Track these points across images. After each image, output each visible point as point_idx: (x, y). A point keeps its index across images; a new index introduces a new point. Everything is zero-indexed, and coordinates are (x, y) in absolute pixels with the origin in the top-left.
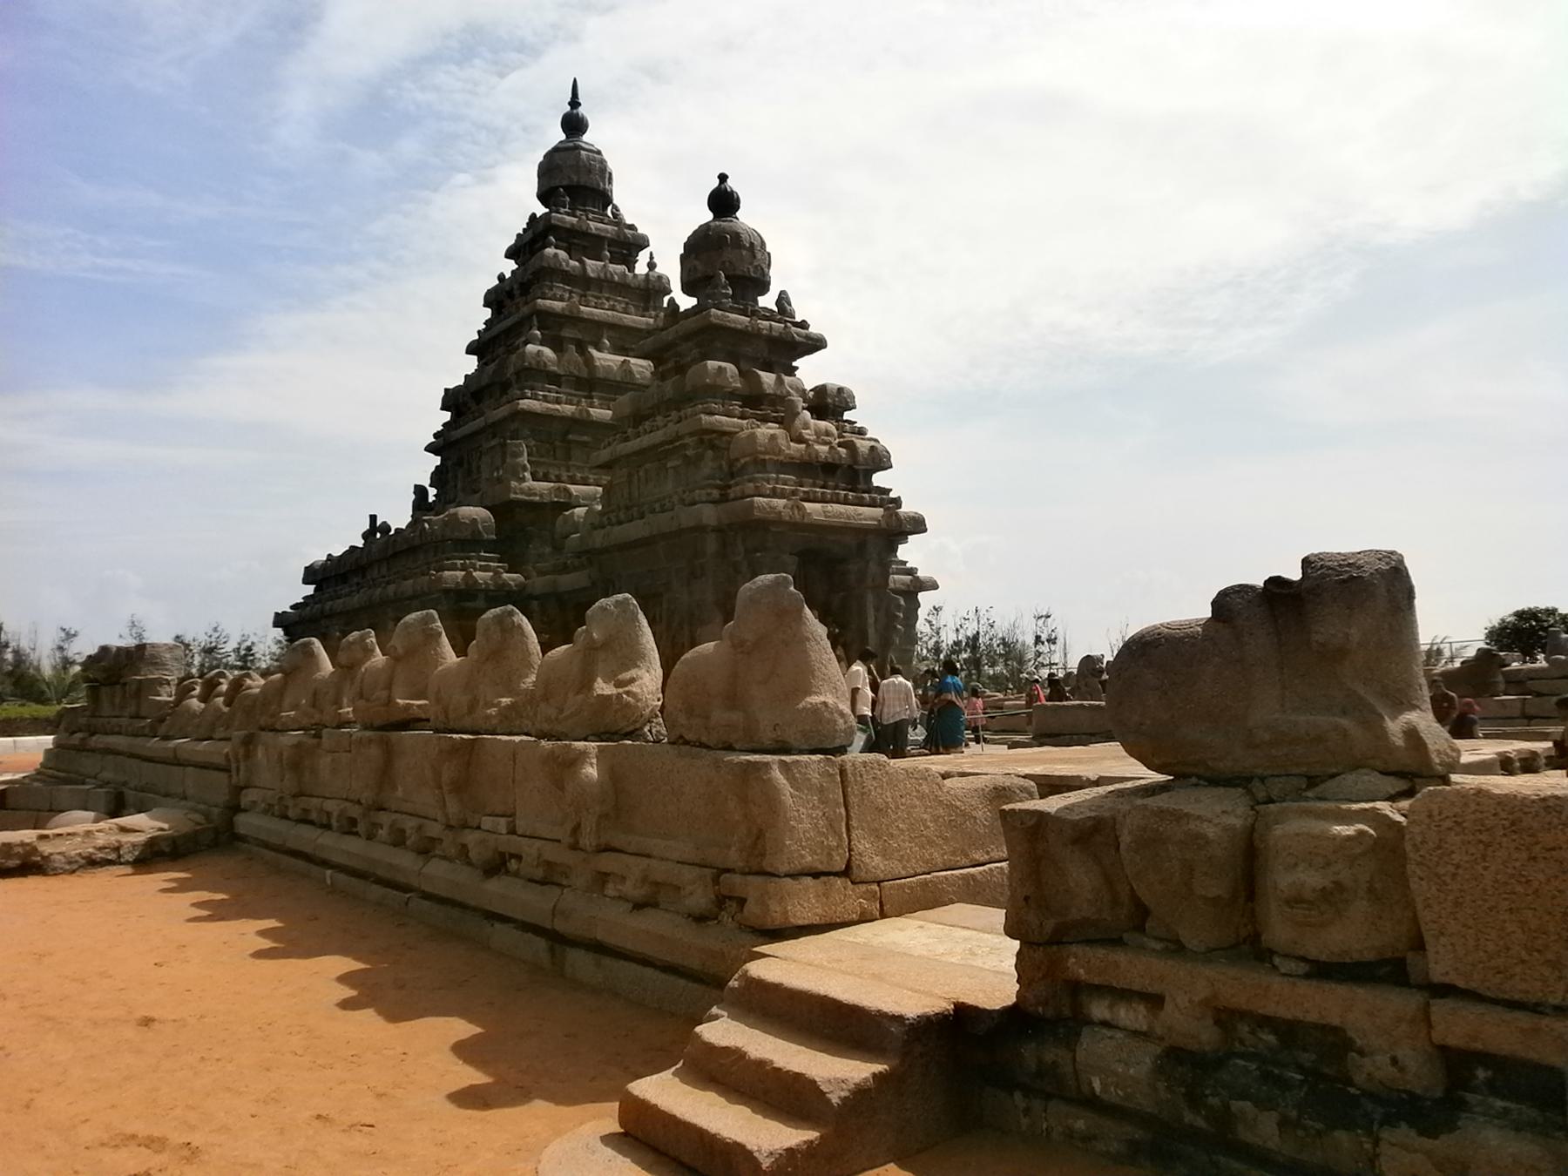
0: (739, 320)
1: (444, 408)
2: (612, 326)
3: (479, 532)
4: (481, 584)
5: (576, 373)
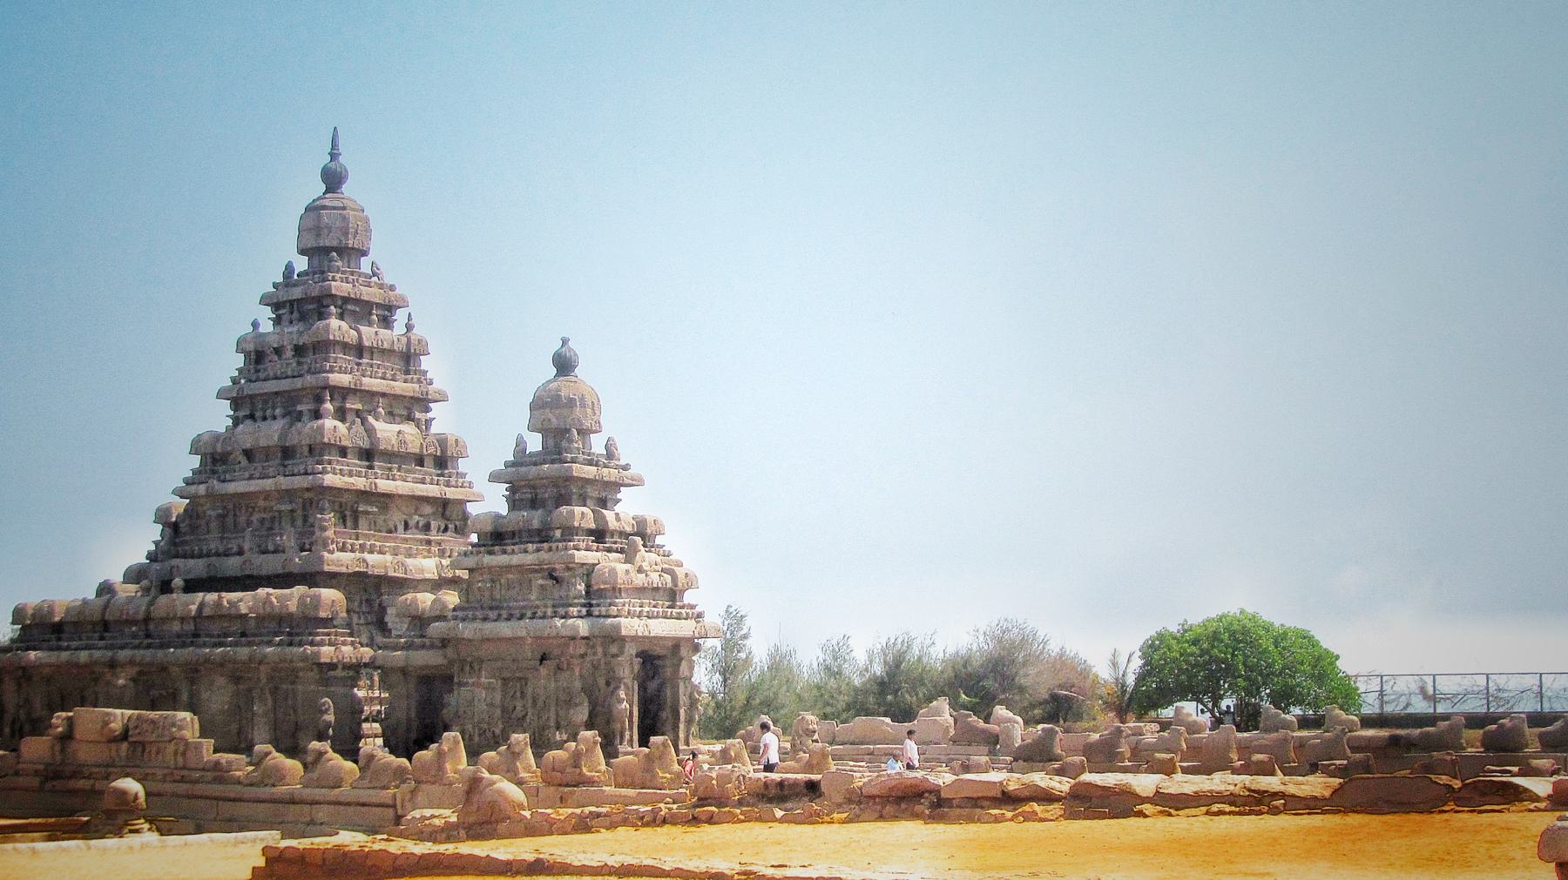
0: (590, 472)
2: (384, 395)
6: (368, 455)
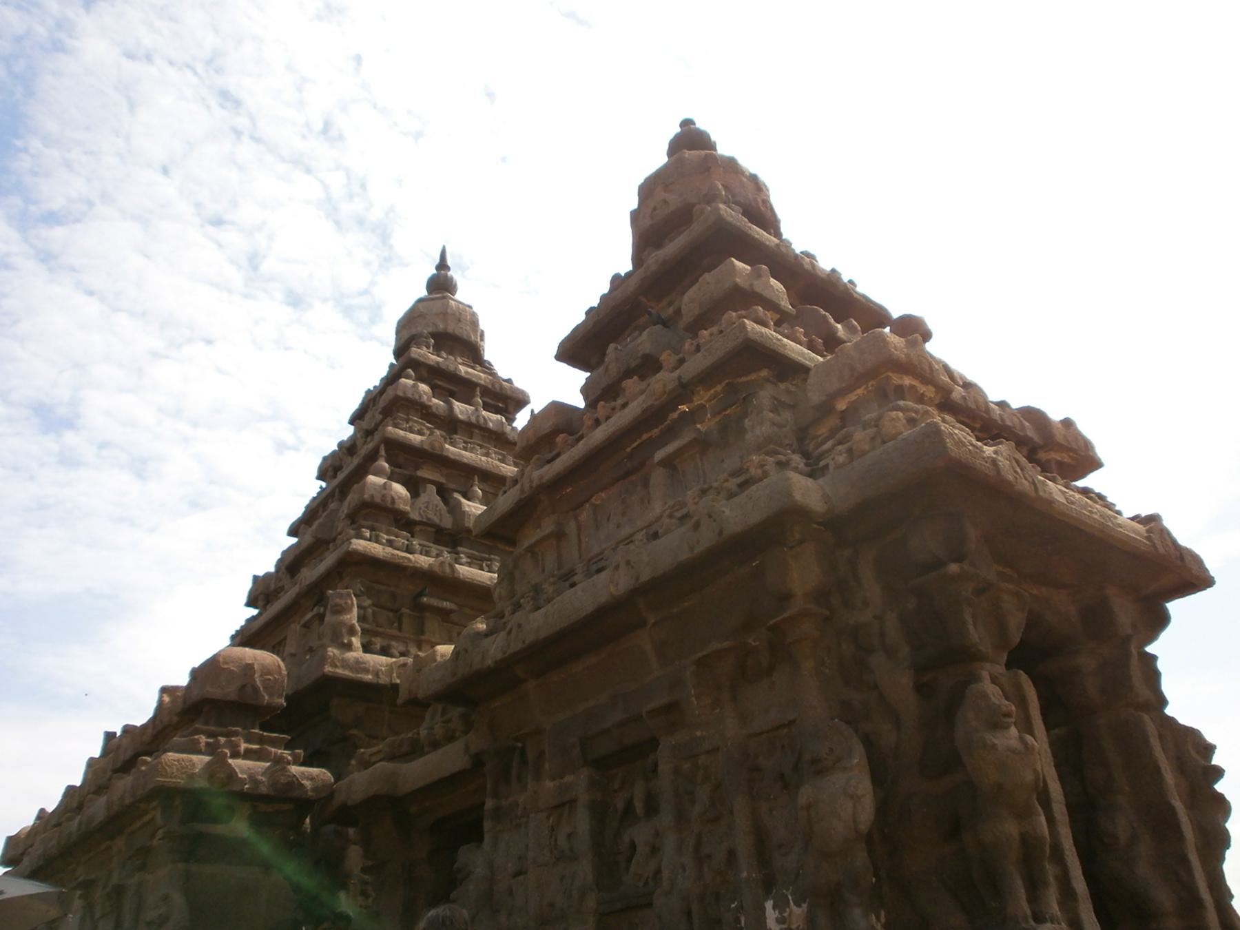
1: (251, 603)
3: (255, 689)
4: (243, 781)
5: (436, 520)
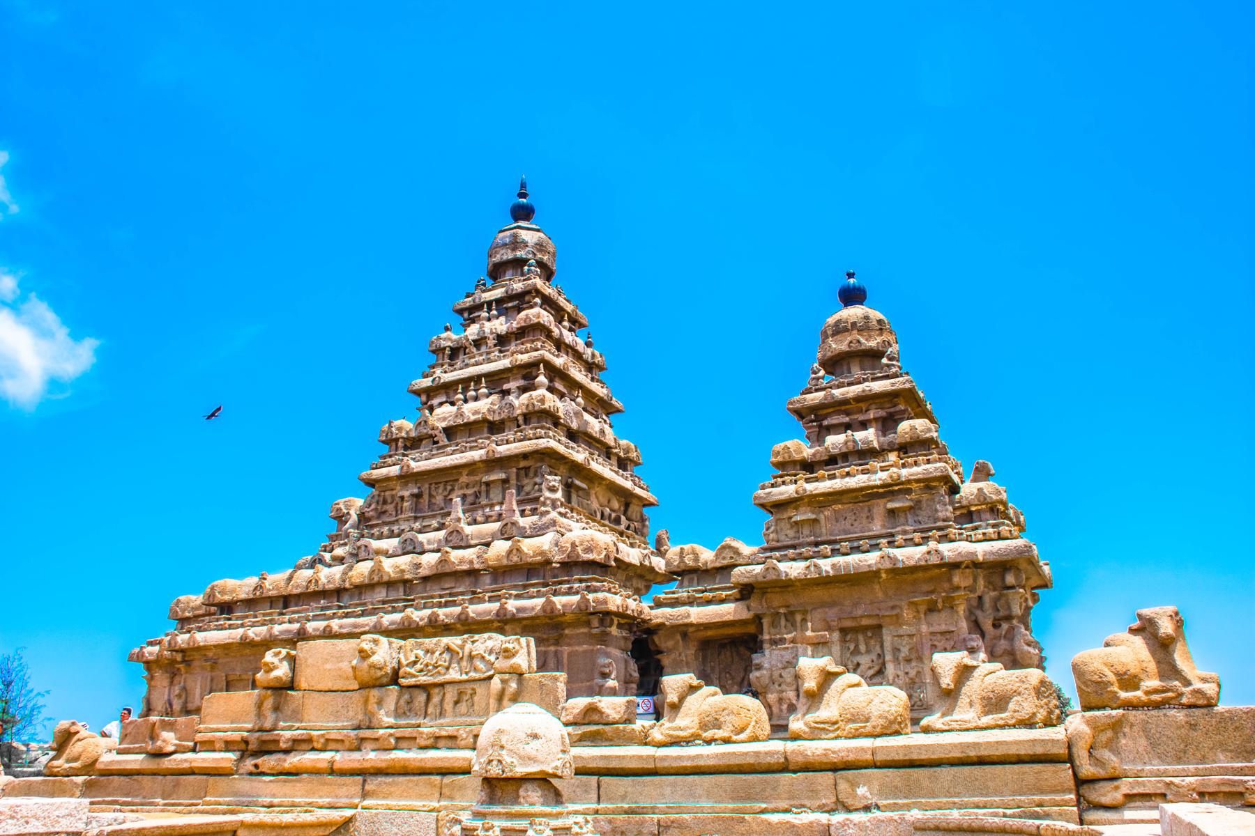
2: (580, 386)
6: (573, 435)
